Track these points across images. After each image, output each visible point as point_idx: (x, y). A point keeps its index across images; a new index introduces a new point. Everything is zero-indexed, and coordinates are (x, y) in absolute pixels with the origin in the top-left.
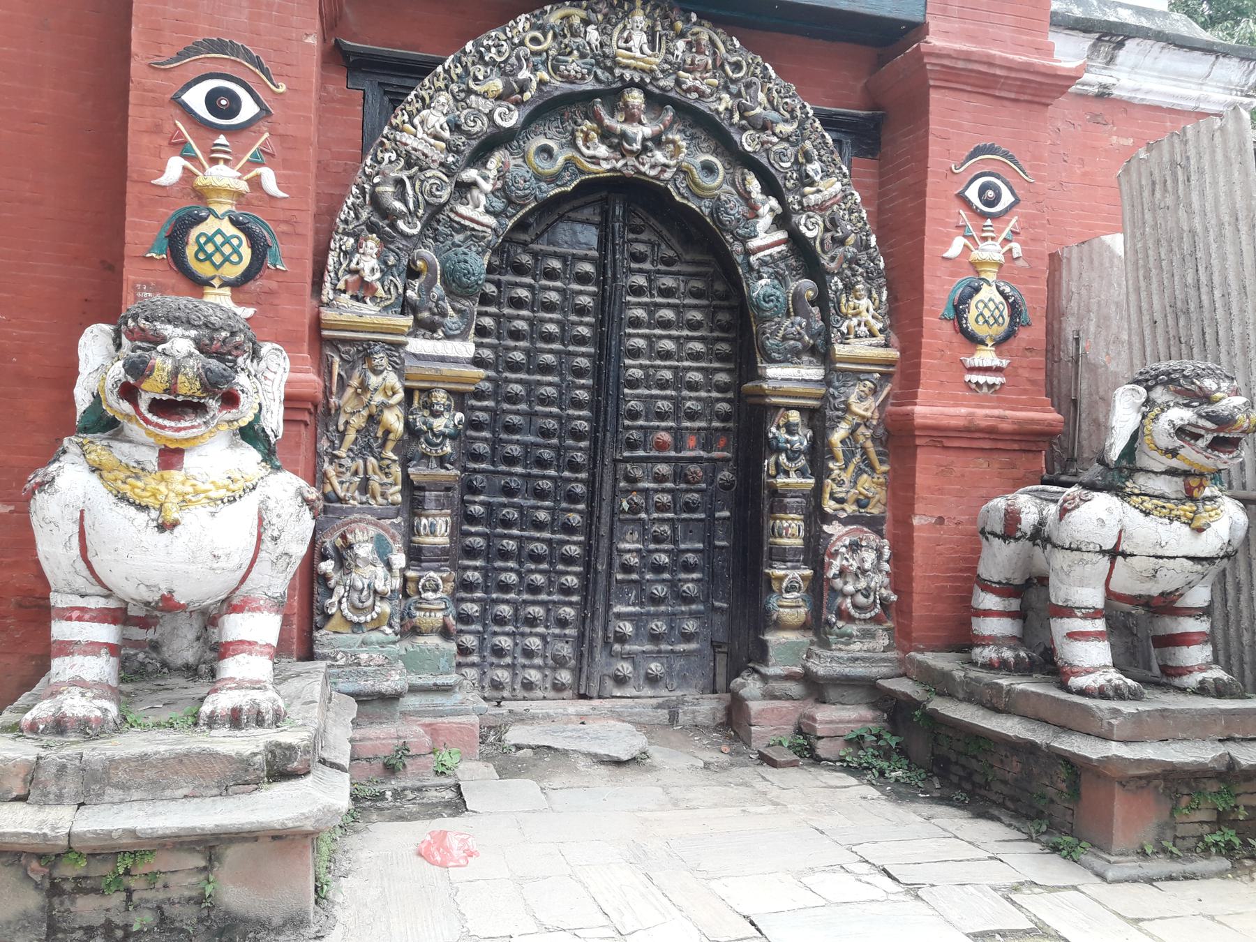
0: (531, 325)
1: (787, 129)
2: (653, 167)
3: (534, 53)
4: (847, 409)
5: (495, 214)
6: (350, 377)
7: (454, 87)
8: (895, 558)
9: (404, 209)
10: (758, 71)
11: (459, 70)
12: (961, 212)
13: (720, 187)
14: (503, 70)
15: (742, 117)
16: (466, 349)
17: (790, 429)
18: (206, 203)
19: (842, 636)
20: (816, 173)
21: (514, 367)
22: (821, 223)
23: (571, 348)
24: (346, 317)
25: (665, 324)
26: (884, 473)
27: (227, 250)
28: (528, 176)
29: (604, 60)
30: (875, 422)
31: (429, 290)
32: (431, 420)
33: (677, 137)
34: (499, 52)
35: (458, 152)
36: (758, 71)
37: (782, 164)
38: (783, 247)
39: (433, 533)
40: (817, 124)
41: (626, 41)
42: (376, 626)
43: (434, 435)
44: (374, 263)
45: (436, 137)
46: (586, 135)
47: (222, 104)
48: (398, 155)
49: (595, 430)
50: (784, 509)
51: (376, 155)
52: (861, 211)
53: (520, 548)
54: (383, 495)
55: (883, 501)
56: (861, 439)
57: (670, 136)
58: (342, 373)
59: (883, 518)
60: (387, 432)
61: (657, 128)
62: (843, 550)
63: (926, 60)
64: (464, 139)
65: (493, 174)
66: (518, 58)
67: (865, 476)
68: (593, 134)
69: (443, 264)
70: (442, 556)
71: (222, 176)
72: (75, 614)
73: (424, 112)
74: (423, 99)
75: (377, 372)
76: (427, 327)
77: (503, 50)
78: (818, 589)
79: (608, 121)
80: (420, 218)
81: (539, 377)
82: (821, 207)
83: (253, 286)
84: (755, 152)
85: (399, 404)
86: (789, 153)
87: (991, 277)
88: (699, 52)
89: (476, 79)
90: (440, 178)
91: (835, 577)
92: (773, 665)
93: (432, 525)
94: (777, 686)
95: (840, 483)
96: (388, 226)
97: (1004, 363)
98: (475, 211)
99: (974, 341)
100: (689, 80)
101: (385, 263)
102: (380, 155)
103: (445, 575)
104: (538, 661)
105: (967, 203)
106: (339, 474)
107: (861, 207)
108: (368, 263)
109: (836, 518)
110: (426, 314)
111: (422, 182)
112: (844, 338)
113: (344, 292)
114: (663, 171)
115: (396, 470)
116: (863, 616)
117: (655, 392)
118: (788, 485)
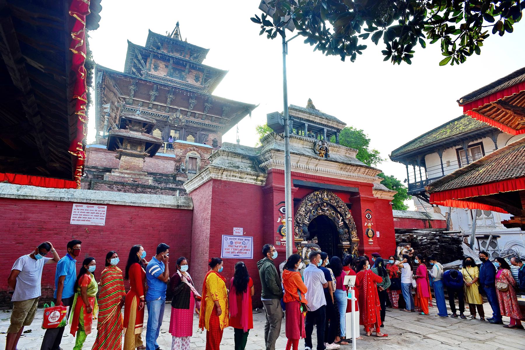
1: (343, 207)
4: (354, 248)
14: (310, 201)
29: (322, 199)
44: (297, 231)
45: (304, 212)
82: (348, 219)
99: (369, 237)
112: (352, 238)
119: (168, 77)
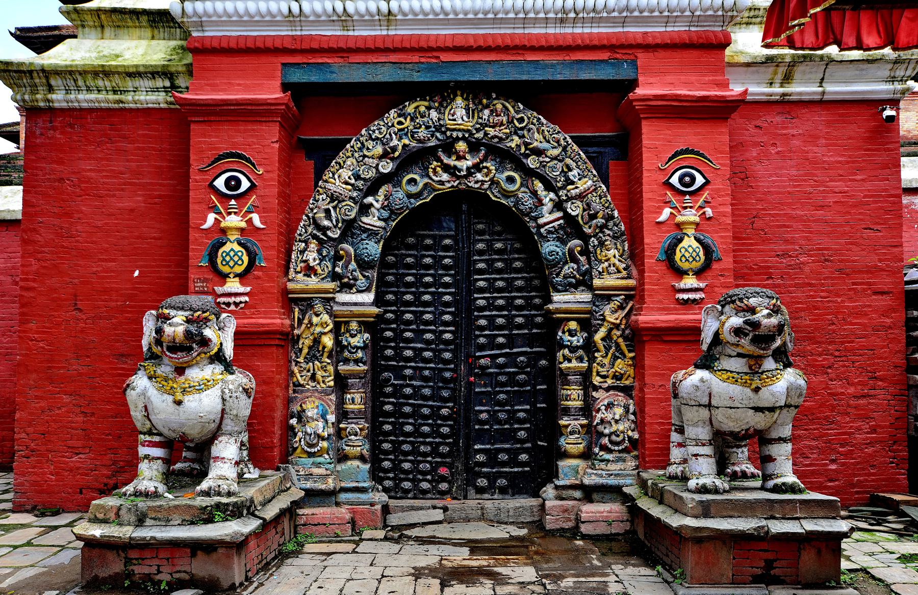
0: (416, 278)
1: (556, 152)
2: (476, 182)
3: (399, 130)
4: (604, 320)
5: (385, 220)
6: (303, 319)
7: (356, 155)
8: (640, 412)
9: (330, 225)
10: (535, 121)
11: (359, 145)
12: (668, 192)
13: (518, 189)
15: (526, 149)
17: (572, 333)
18: (226, 235)
19: (602, 461)
20: (575, 177)
21: (408, 304)
22: (580, 206)
23: (440, 290)
24: (299, 286)
25: (499, 271)
26: (631, 358)
27: (236, 258)
28: (401, 197)
30: (623, 327)
31: (347, 267)
32: (350, 339)
33: (488, 165)
34: (380, 132)
35: (360, 190)
36: (535, 121)
37: (555, 174)
38: (561, 221)
39: (353, 402)
40: (575, 147)
41: (453, 116)
42: (319, 454)
43: (351, 347)
44: (315, 255)
45: (346, 183)
46: (434, 169)
47: (233, 183)
48: (327, 196)
49: (455, 338)
50: (568, 383)
51: (315, 197)
52: (606, 196)
53: (414, 411)
54: (323, 382)
55: (632, 375)
56: (615, 338)
57: (484, 164)
58: (301, 317)
59: (632, 386)
60: (324, 347)
61: (476, 161)
62: (603, 408)
63: (634, 104)
64: (362, 182)
65: (381, 198)
66: (390, 135)
67: (619, 360)
68: (438, 169)
69: (355, 250)
71: (233, 221)
72: (147, 443)
73: (340, 171)
74: (340, 164)
75: (317, 315)
76: (346, 287)
77: (382, 131)
78: (592, 432)
79: (446, 160)
80: (340, 229)
81: (421, 309)
82: (581, 197)
83: (250, 276)
84: (536, 168)
85: (331, 331)
86: (558, 167)
87: (691, 231)
88: (497, 116)
89: (368, 149)
90: (350, 205)
91: (598, 424)
92: (563, 479)
93: (353, 399)
94: (565, 493)
95: (602, 366)
96: (322, 234)
97: (702, 285)
99: (680, 273)
100: (491, 132)
101: (321, 254)
102: (317, 197)
103: (361, 426)
104: (429, 477)
105: (672, 187)
106: (300, 372)
107: (607, 194)
108: (312, 256)
109: (601, 387)
110: (346, 280)
111: (340, 208)
113: (300, 273)
114: (483, 184)
115: (331, 368)
116: (616, 448)
117: (494, 313)
118: (569, 368)
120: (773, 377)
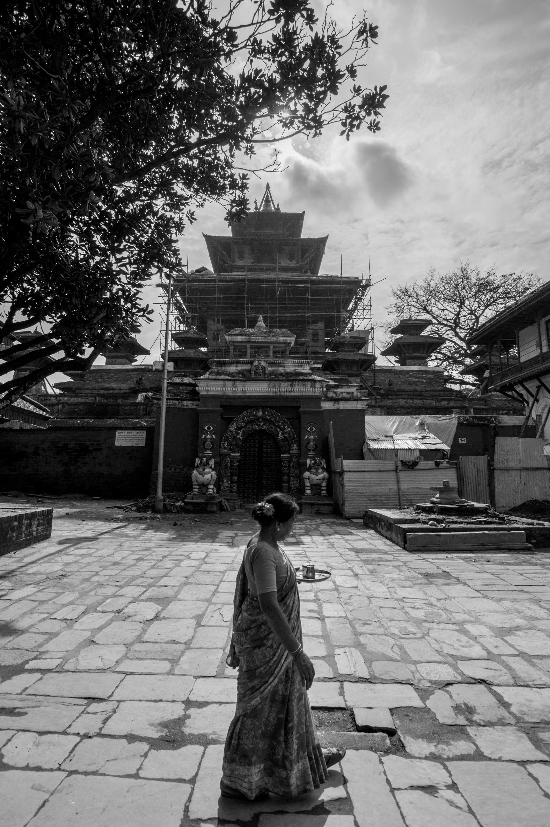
16: (238, 454)
29: (256, 415)
47: (209, 428)
70: (235, 482)
71: (209, 436)
76: (233, 452)
98: (240, 437)
99: (309, 450)
108: (226, 445)
119: (256, 264)
120: (321, 473)
